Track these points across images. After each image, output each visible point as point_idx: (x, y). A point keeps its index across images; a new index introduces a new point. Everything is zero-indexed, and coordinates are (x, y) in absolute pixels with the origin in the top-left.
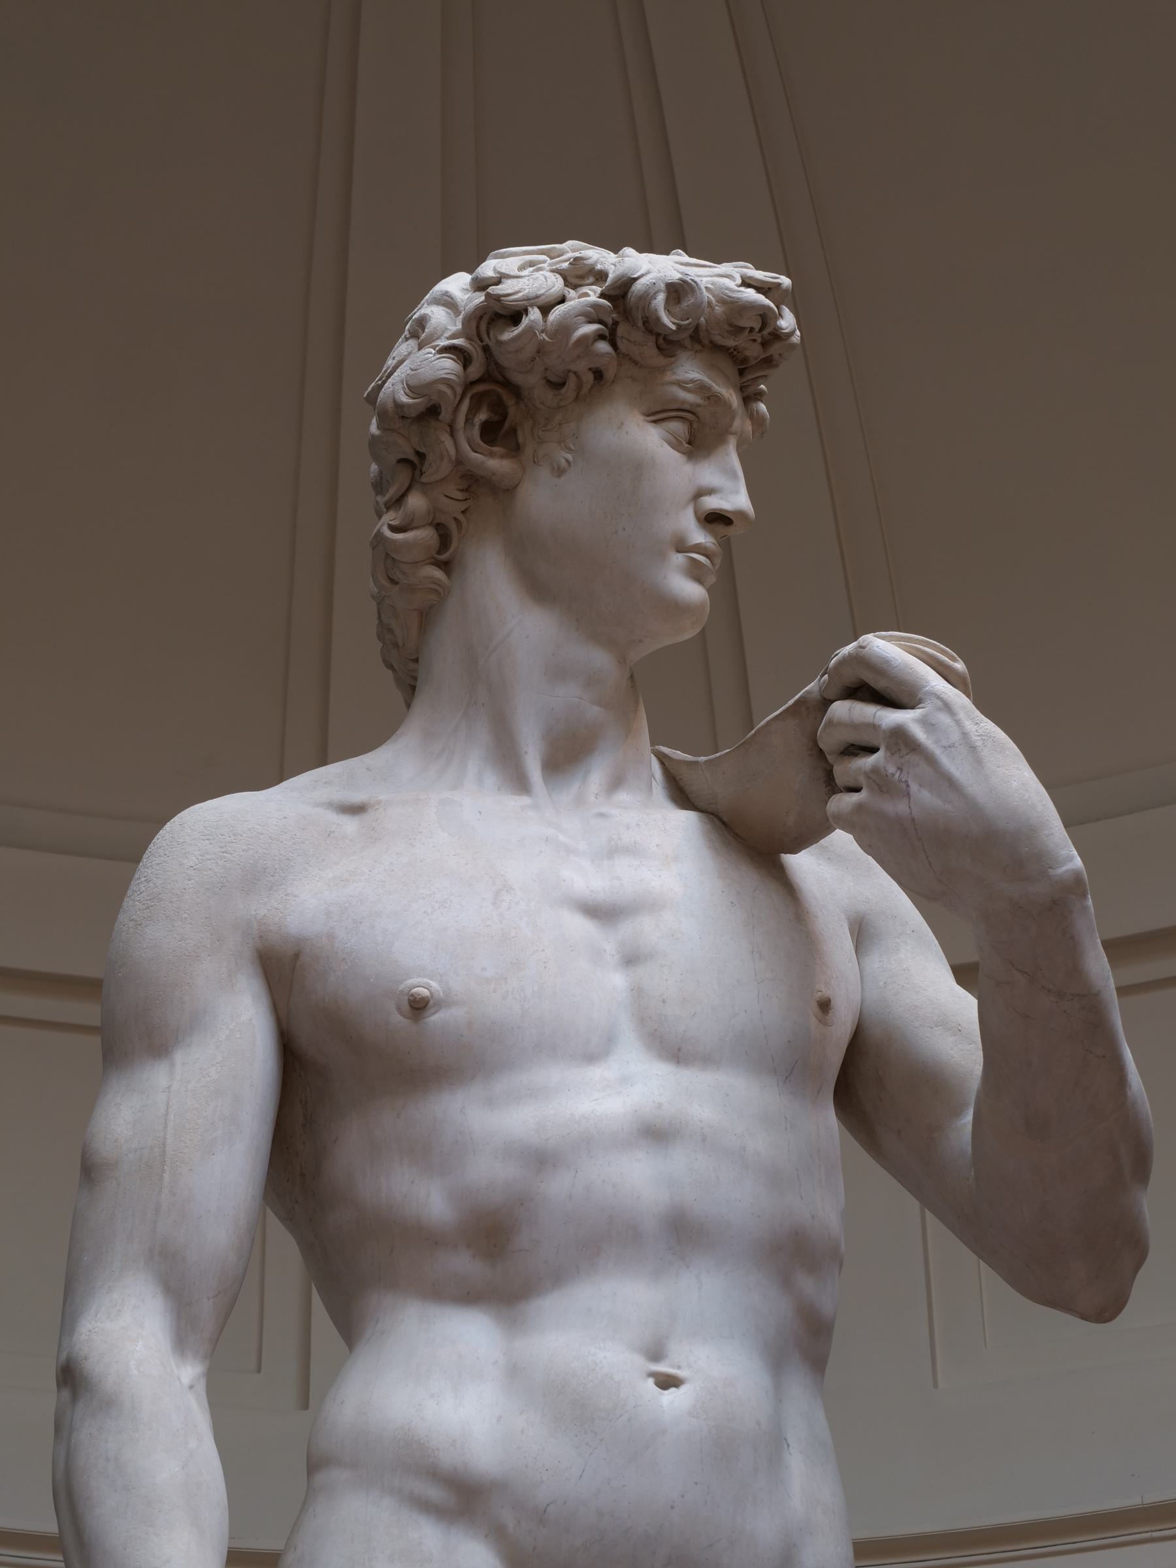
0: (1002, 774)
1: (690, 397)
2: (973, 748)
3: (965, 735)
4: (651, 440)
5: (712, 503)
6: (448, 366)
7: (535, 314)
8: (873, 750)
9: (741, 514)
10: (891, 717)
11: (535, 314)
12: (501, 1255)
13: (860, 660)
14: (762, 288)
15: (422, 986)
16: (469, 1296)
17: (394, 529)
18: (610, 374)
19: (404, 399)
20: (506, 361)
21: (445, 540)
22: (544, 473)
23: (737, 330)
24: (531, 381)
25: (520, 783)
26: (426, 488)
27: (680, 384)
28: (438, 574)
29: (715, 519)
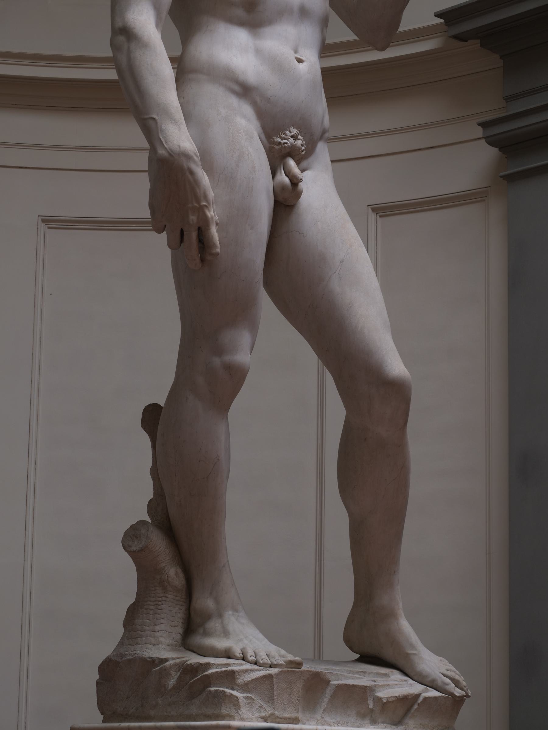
16: (241, 23)
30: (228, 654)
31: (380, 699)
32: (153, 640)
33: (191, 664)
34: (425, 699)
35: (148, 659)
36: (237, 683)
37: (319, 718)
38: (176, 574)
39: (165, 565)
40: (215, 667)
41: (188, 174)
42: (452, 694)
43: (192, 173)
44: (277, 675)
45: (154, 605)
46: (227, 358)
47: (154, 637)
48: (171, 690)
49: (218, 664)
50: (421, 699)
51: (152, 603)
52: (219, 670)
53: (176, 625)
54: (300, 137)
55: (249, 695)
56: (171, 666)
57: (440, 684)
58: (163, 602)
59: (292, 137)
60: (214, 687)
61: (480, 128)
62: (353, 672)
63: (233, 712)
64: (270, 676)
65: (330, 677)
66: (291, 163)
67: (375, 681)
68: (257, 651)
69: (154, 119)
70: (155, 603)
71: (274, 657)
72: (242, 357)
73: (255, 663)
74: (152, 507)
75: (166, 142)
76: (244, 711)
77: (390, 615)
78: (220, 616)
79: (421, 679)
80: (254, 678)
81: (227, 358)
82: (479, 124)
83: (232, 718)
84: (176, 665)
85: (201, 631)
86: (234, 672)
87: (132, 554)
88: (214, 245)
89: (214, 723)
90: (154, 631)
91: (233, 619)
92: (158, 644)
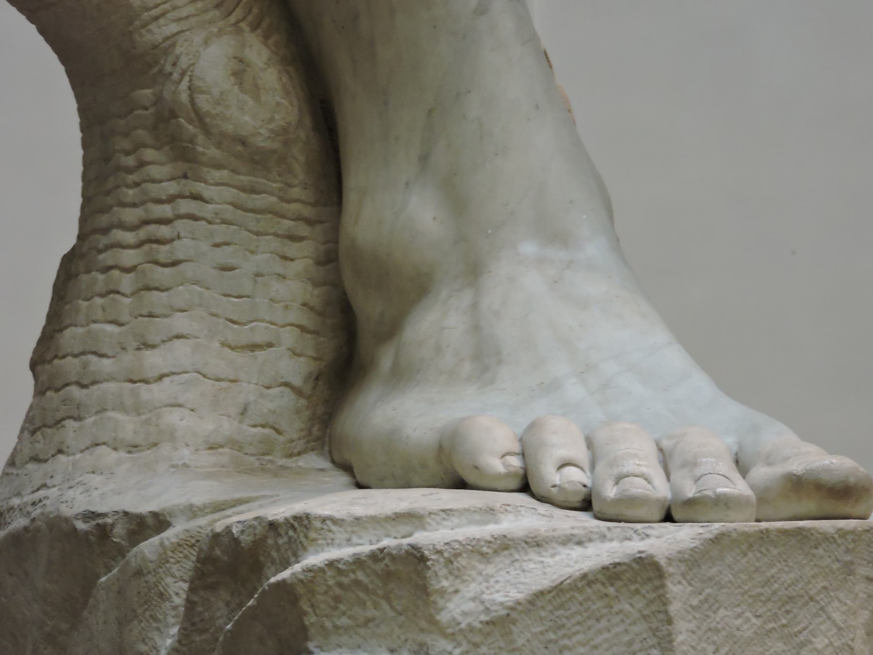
35: (81, 525)
36: (443, 617)
38: (240, 71)
39: (174, 28)
40: (340, 534)
44: (691, 560)
45: (139, 245)
47: (137, 410)
51: (129, 237)
52: (345, 552)
53: (259, 339)
58: (181, 225)
70: (143, 233)
73: (586, 505)
80: (545, 583)
86: (423, 559)
91: (533, 282)
92: (155, 445)
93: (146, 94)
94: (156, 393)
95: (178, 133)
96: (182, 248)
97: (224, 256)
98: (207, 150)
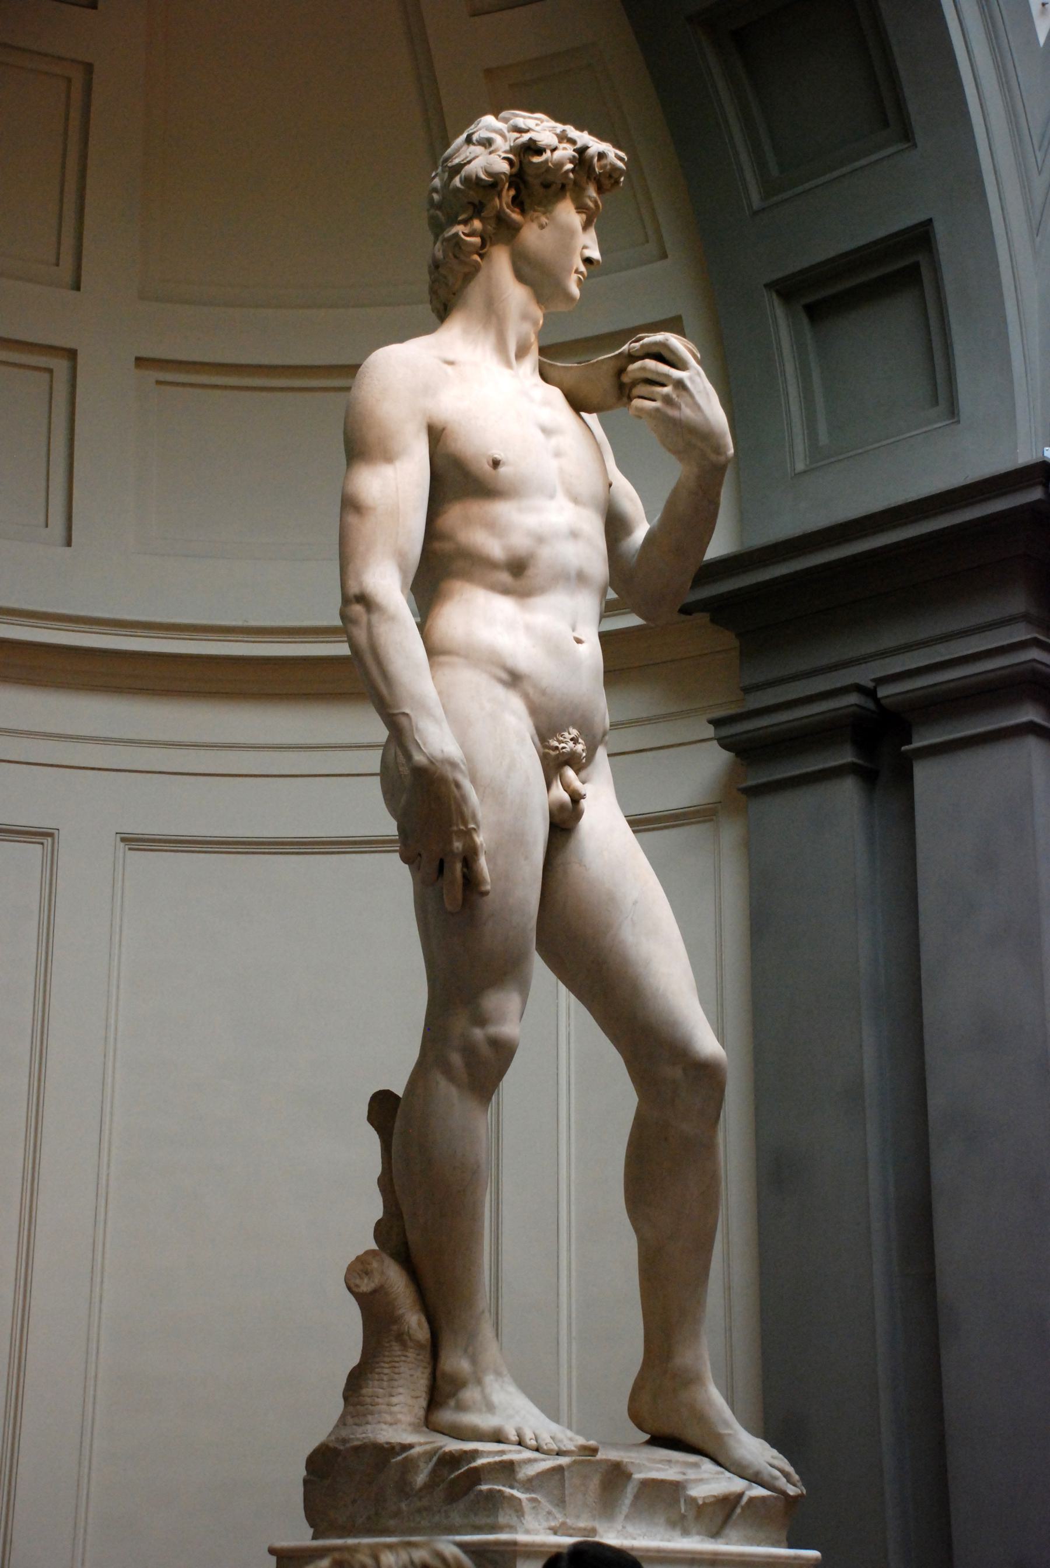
0: (709, 406)
1: (591, 204)
2: (707, 394)
3: (705, 388)
4: (576, 220)
5: (588, 253)
6: (505, 167)
7: (549, 152)
8: (663, 385)
9: (598, 261)
10: (676, 373)
11: (549, 152)
12: (518, 575)
13: (664, 345)
14: (621, 159)
15: (499, 455)
17: (464, 234)
18: (567, 188)
19: (483, 177)
20: (529, 171)
21: (483, 245)
22: (535, 226)
23: (610, 176)
24: (535, 182)
25: (509, 365)
26: (482, 220)
27: (590, 197)
28: (478, 258)
29: (588, 261)
30: (498, 1437)
31: (693, 1500)
32: (388, 1418)
33: (450, 1452)
34: (752, 1499)
37: (620, 1528)
38: (419, 1324)
41: (453, 787)
42: (784, 1493)
43: (458, 785)
44: (570, 1466)
46: (493, 1030)
47: (391, 1413)
48: (421, 1490)
49: (488, 1453)
50: (745, 1499)
51: (387, 1365)
54: (580, 740)
55: (533, 1496)
56: (420, 1455)
57: (766, 1478)
58: (401, 1364)
59: (572, 739)
60: (485, 1484)
61: (711, 728)
62: (654, 1461)
63: (514, 1521)
64: (559, 1470)
65: (631, 1469)
66: (570, 773)
67: (684, 1474)
68: (537, 1432)
69: (407, 715)
71: (561, 1441)
72: (509, 1029)
73: (537, 1450)
74: (381, 1231)
75: (425, 744)
76: (530, 1521)
77: (690, 1380)
78: (479, 1382)
79: (740, 1470)
81: (493, 1030)
82: (710, 722)
83: (512, 1528)
84: (425, 1453)
85: (452, 1403)
87: (361, 1298)
88: (484, 881)
89: (491, 1537)
90: (389, 1405)
91: (496, 1386)
93: (395, 1327)
94: (396, 1409)
95: (402, 1338)
96: (402, 1369)
97: (412, 1372)
98: (410, 1344)
